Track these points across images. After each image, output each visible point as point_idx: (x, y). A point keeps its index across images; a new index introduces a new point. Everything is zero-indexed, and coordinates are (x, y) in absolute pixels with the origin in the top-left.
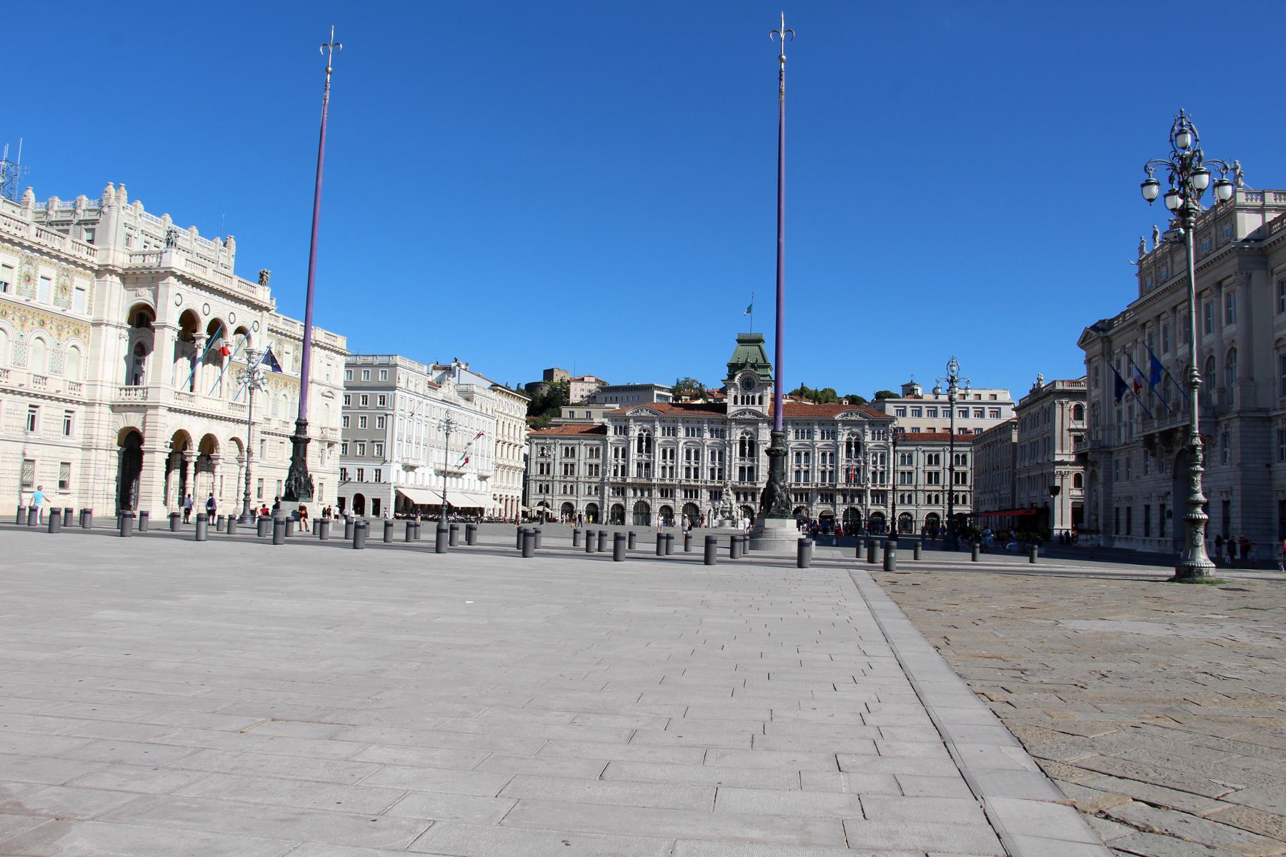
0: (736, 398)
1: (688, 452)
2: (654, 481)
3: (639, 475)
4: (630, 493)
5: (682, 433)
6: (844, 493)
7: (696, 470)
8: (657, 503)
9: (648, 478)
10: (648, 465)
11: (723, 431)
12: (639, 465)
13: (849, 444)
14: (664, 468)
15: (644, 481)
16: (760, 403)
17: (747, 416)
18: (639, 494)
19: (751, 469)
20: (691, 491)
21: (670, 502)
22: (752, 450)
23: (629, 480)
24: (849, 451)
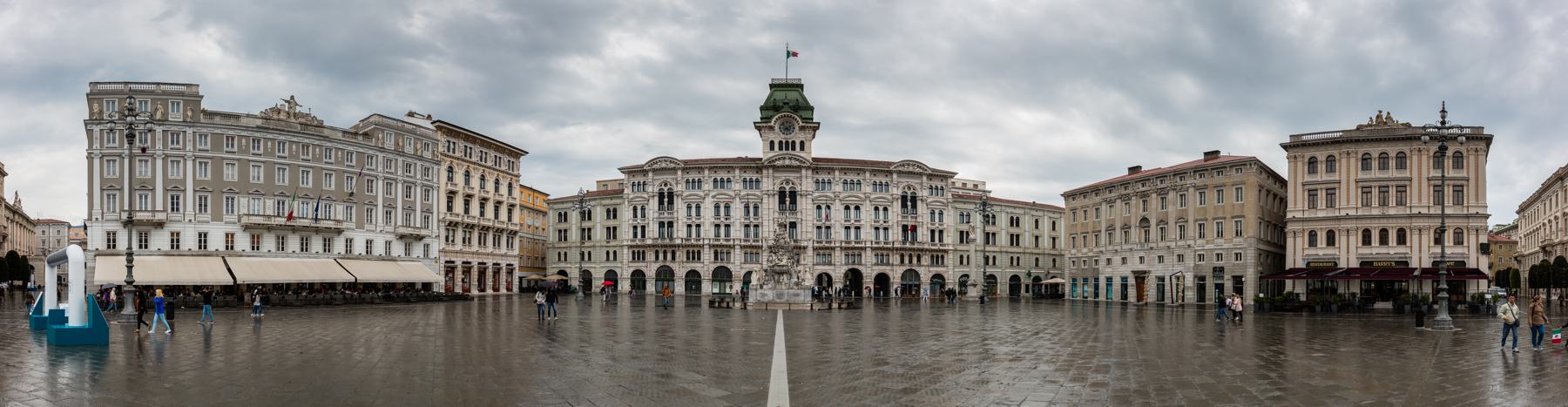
0: (772, 143)
1: (717, 207)
2: (678, 242)
3: (661, 235)
4: (650, 256)
5: (708, 186)
6: (901, 252)
7: (727, 226)
8: (680, 270)
9: (671, 238)
10: (671, 224)
11: (757, 181)
12: (661, 225)
13: (904, 198)
14: (689, 226)
15: (667, 241)
16: (802, 148)
17: (787, 162)
18: (661, 256)
19: (793, 225)
20: (720, 251)
21: (697, 266)
22: (794, 202)
23: (649, 242)
24: (904, 205)
